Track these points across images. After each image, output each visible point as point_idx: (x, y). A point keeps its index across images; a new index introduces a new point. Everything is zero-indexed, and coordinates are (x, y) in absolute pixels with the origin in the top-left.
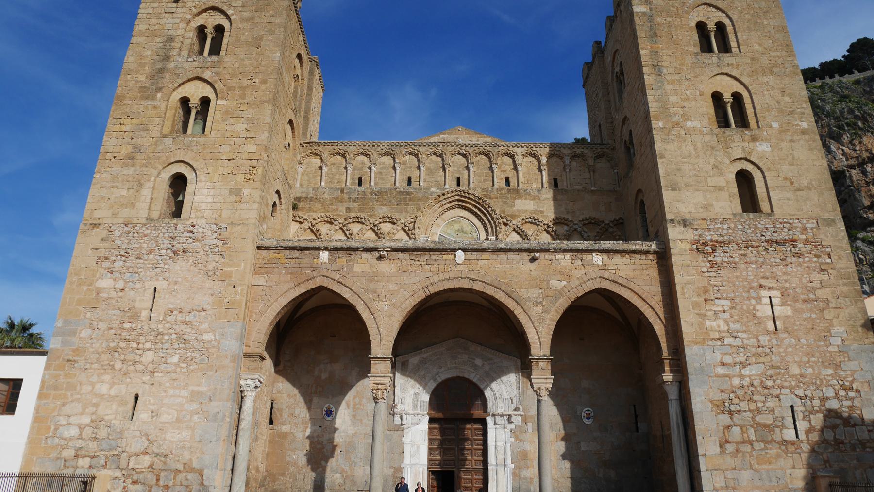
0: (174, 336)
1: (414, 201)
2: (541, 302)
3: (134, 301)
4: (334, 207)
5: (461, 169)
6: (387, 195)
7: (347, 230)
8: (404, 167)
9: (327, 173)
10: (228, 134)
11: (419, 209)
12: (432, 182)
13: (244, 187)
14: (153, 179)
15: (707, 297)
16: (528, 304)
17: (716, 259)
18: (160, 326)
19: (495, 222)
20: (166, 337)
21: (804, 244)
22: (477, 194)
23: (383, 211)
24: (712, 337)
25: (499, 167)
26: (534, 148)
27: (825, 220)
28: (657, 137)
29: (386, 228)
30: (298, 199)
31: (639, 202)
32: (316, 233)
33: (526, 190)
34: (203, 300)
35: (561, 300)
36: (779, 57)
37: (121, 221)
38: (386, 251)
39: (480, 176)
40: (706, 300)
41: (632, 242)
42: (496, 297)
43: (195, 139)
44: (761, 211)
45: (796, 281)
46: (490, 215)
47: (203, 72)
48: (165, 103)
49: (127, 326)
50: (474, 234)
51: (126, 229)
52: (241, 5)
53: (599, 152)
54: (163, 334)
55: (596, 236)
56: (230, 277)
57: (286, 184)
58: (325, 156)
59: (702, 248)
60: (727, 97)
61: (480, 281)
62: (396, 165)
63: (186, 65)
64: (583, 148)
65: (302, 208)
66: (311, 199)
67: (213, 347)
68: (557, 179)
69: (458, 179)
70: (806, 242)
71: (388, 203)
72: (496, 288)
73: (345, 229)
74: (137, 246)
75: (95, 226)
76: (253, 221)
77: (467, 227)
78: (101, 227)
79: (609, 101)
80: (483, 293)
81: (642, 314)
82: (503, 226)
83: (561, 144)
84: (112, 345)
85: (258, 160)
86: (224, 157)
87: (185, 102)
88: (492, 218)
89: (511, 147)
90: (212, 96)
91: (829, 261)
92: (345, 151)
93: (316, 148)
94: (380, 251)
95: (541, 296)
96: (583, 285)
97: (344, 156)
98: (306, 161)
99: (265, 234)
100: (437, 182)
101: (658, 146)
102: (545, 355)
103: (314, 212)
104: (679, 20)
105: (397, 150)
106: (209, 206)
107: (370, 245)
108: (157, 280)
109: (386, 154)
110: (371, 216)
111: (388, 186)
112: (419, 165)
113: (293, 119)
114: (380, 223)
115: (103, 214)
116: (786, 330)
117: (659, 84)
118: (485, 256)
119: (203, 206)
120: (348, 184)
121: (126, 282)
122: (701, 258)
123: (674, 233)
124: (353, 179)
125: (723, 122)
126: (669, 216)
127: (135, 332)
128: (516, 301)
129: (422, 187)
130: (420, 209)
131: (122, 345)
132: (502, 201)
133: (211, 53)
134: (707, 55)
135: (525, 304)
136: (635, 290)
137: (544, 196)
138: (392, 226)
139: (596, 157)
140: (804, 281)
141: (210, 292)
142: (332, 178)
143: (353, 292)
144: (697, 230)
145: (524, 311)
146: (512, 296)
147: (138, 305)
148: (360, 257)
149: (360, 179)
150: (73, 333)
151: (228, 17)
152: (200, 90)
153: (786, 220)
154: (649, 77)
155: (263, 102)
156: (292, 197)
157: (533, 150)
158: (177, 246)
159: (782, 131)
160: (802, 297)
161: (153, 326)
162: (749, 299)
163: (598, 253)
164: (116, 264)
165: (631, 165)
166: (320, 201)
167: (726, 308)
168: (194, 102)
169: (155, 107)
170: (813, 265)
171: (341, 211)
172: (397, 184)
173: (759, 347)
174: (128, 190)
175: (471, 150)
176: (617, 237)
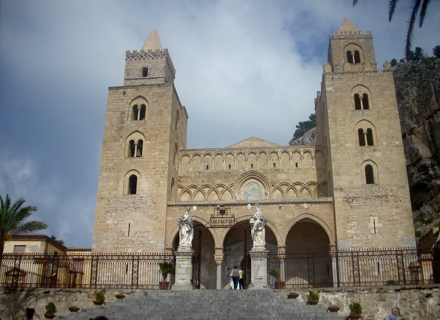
0: (139, 242)
3: (122, 229)
4: (197, 181)
5: (253, 160)
10: (152, 157)
13: (160, 180)
14: (123, 177)
15: (348, 221)
16: (277, 225)
17: (353, 204)
18: (133, 238)
20: (136, 243)
21: (391, 197)
22: (260, 172)
24: (349, 236)
27: (401, 186)
28: (332, 151)
33: (282, 169)
34: (149, 227)
36: (390, 110)
37: (112, 196)
40: (347, 222)
43: (138, 159)
44: (375, 183)
45: (386, 212)
47: (139, 128)
48: (124, 144)
49: (120, 238)
51: (115, 199)
52: (152, 95)
54: (135, 242)
56: (158, 218)
59: (348, 200)
60: (365, 131)
63: (131, 125)
66: (186, 177)
67: (154, 246)
69: (252, 165)
70: (392, 196)
74: (120, 206)
75: (102, 198)
76: (166, 195)
78: (105, 199)
82: (272, 187)
84: (116, 246)
86: (151, 167)
87: (132, 142)
90: (143, 139)
91: (400, 203)
93: (187, 152)
98: (183, 158)
101: (333, 156)
102: (283, 246)
104: (346, 94)
105: (224, 152)
106: (147, 189)
108: (130, 220)
110: (213, 184)
111: (220, 169)
114: (217, 187)
115: (105, 193)
116: (379, 233)
119: (145, 189)
121: (118, 221)
122: (347, 204)
123: (337, 194)
125: (362, 143)
126: (335, 187)
127: (124, 241)
131: (119, 246)
133: (141, 119)
134: (357, 111)
135: (275, 225)
137: (291, 172)
140: (389, 212)
141: (151, 224)
144: (346, 192)
147: (124, 230)
149: (207, 166)
150: (100, 242)
151: (147, 100)
152: (138, 136)
153: (384, 187)
158: (136, 206)
159: (387, 146)
160: (387, 219)
161: (130, 238)
162: (365, 221)
164: (113, 214)
167: (355, 225)
168: (136, 142)
169: (120, 145)
170: (394, 206)
173: (367, 240)
174: (114, 183)
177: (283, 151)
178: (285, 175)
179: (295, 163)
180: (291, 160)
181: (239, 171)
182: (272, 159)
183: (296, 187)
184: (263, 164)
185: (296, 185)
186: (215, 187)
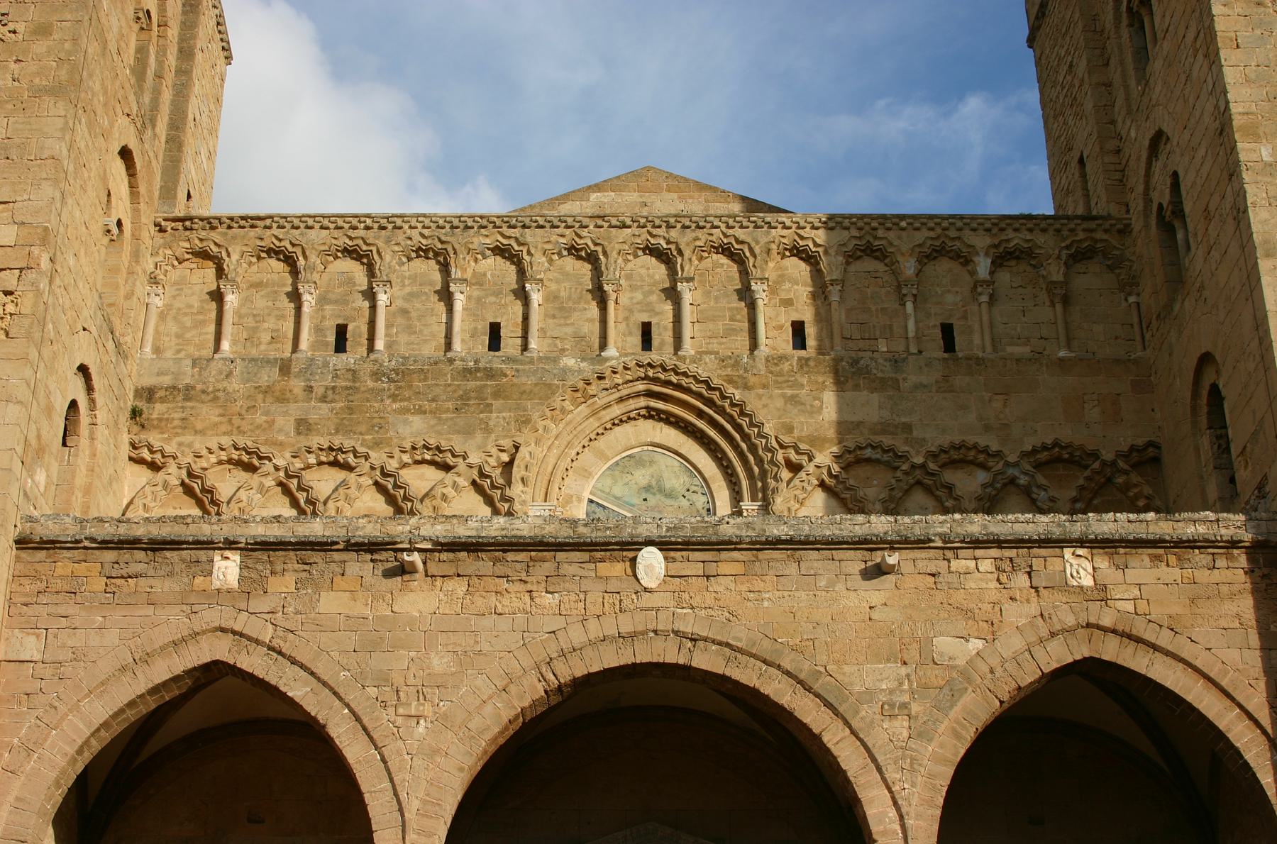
1: (507, 398)
2: (904, 706)
4: (260, 419)
6: (425, 379)
7: (300, 488)
8: (476, 293)
9: (237, 313)
11: (525, 422)
12: (562, 339)
16: (865, 711)
19: (760, 462)
22: (703, 375)
23: (414, 428)
25: (773, 291)
26: (880, 233)
29: (420, 479)
30: (148, 394)
31: (1205, 393)
32: (205, 498)
33: (855, 362)
35: (968, 698)
38: (420, 550)
39: (713, 319)
41: (1186, 515)
42: (767, 690)
46: (746, 437)
50: (694, 497)
53: (1080, 241)
55: (1075, 500)
57: (110, 345)
58: (230, 263)
61: (713, 642)
62: (453, 288)
64: (1030, 230)
65: (160, 420)
66: (188, 393)
68: (951, 325)
69: (646, 330)
71: (427, 406)
72: (765, 661)
73: (293, 484)
77: (676, 478)
79: (1108, 85)
80: (724, 679)
81: (1220, 736)
83: (961, 217)
85: (21, 270)
88: (753, 448)
89: (809, 226)
92: (293, 245)
93: (203, 234)
94: (403, 550)
95: (906, 686)
96: (1039, 652)
97: (290, 261)
99: (41, 501)
100: (579, 338)
103: (196, 432)
105: (457, 239)
107: (369, 531)
109: (422, 252)
110: (377, 444)
112: (524, 287)
113: (133, 145)
114: (404, 466)
117: (1258, 32)
118: (730, 564)
120: (304, 344)
124: (318, 330)
128: (828, 705)
129: (535, 355)
130: (527, 421)
132: (784, 396)
136: (1198, 663)
137: (913, 379)
138: (439, 475)
139: (1071, 256)
142: (255, 330)
143: (319, 679)
145: (853, 732)
146: (816, 687)
148: (339, 570)
149: (341, 332)
154: (1226, 10)
155: (37, 93)
156: (130, 387)
157: (876, 238)
163: (1080, 551)
165: (1176, 279)
166: (216, 399)
171: (280, 430)
172: (457, 346)
175: (684, 239)
176: (1141, 503)
177: (856, 248)
178: (875, 395)
179: (936, 321)
180: (909, 306)
181: (555, 360)
182: (784, 295)
183: (949, 476)
184: (720, 327)
185: (953, 464)
186: (392, 465)
